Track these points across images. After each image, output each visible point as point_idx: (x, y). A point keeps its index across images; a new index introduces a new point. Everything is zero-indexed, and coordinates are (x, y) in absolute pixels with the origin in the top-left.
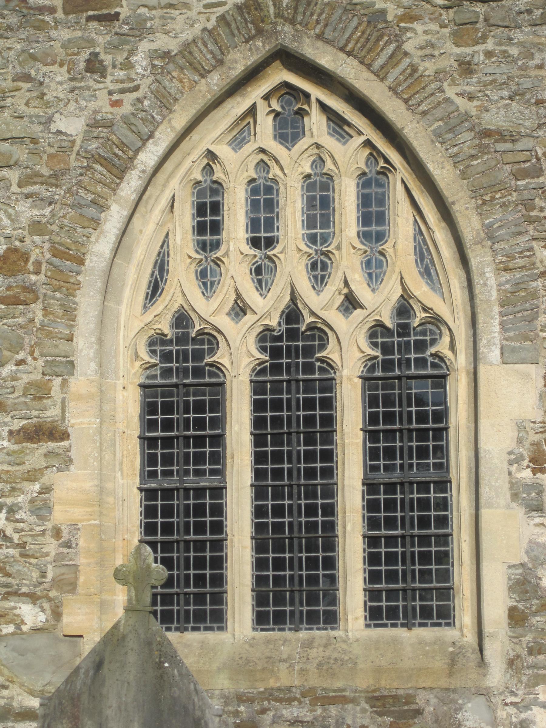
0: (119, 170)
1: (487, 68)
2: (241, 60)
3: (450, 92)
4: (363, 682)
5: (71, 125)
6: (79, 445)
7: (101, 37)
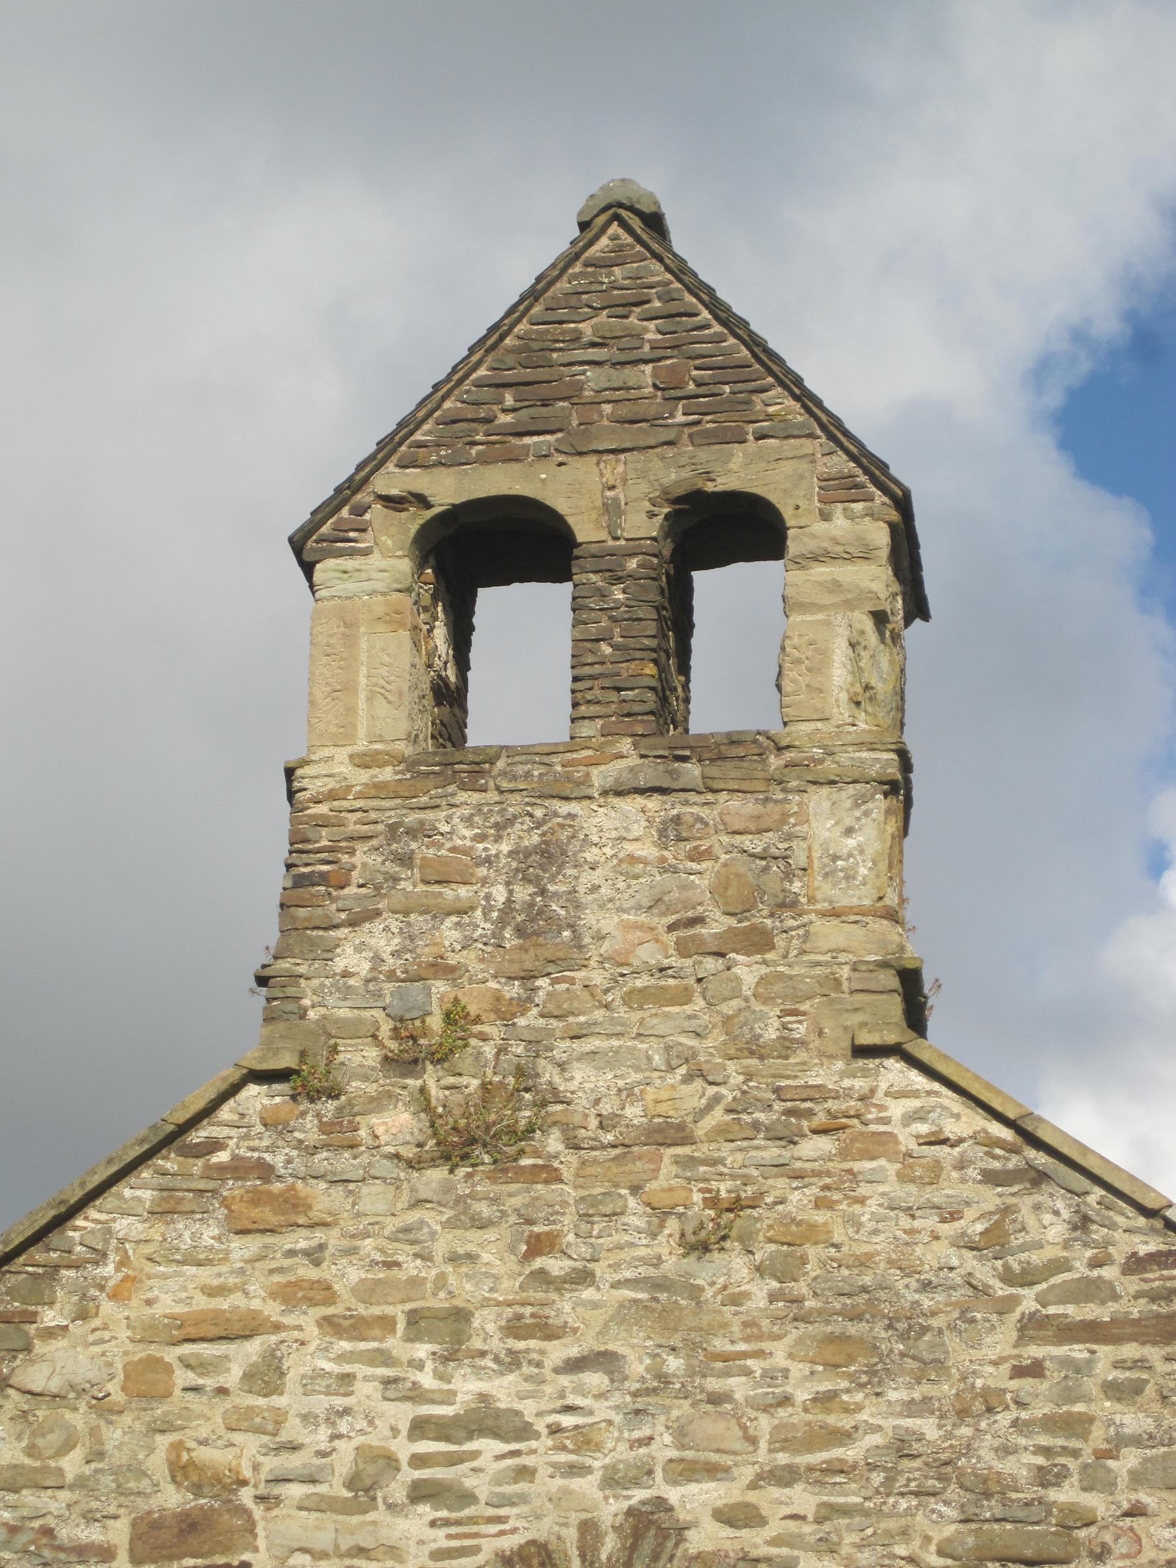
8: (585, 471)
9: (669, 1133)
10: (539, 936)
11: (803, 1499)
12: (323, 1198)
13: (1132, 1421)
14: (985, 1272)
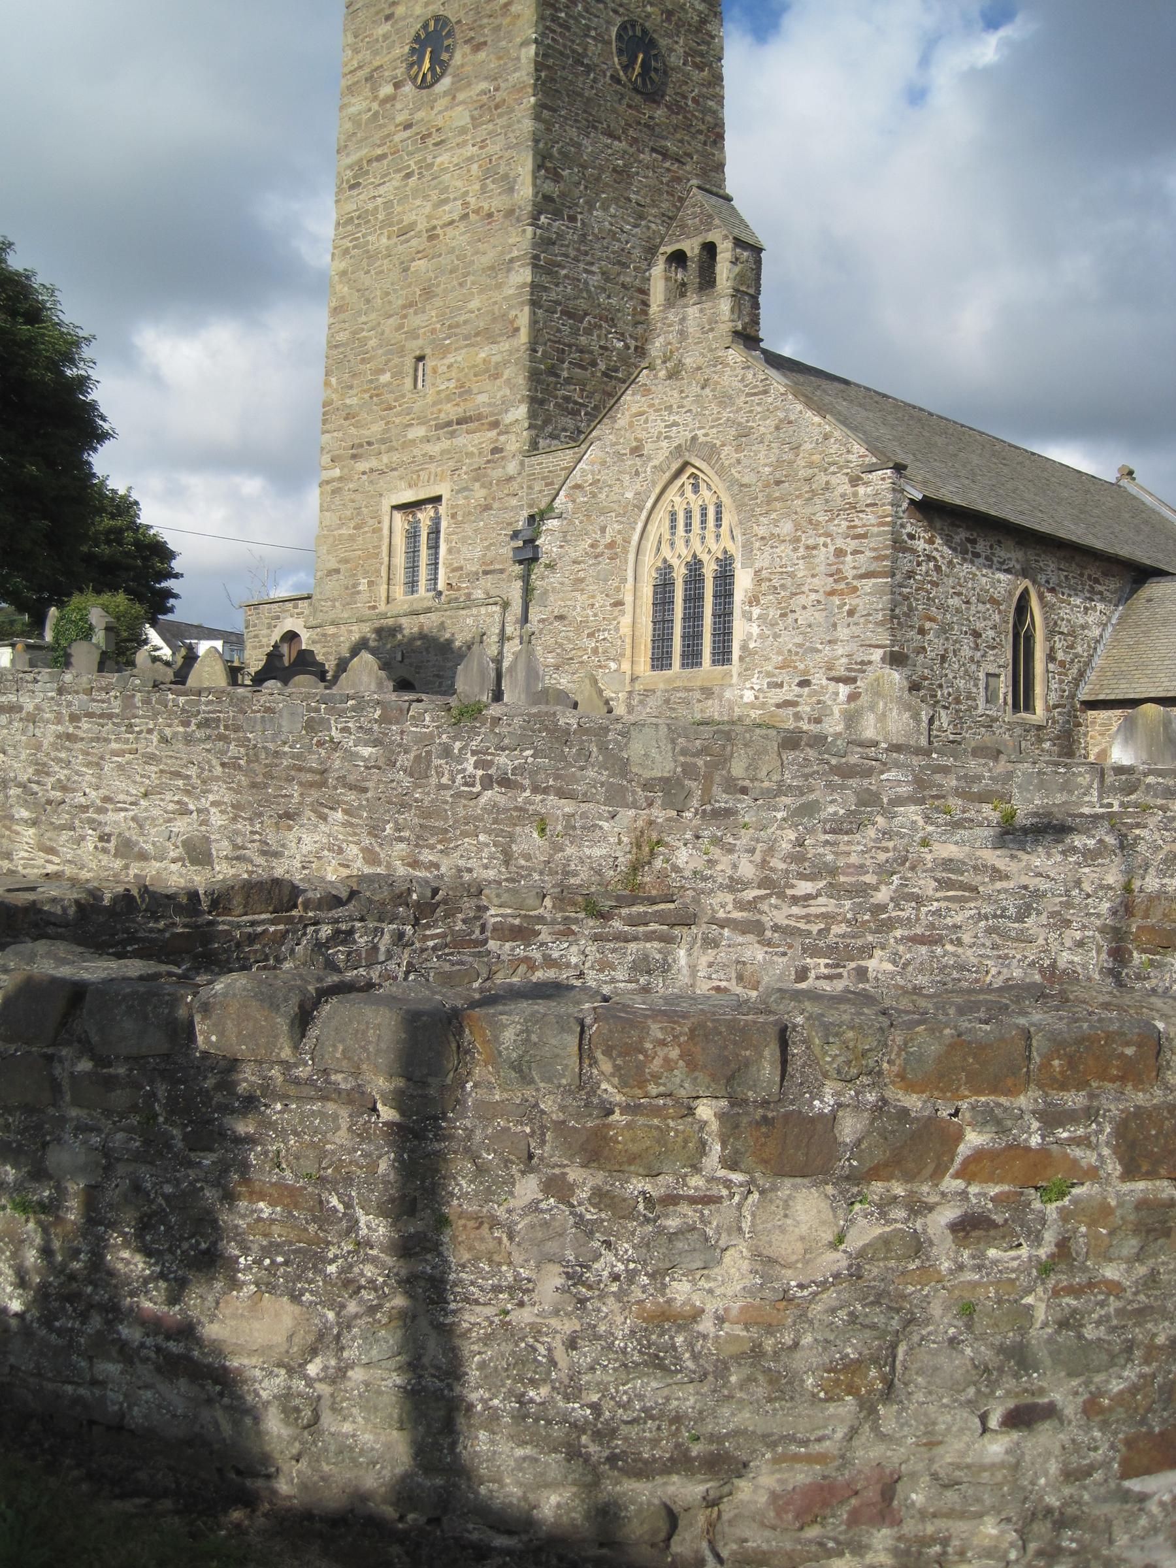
0: (641, 510)
1: (745, 462)
2: (675, 466)
3: (733, 471)
4: (699, 684)
5: (629, 495)
6: (628, 607)
7: (638, 462)
8: (689, 241)
9: (699, 368)
10: (682, 334)
11: (715, 430)
12: (653, 388)
13: (759, 409)
14: (740, 385)
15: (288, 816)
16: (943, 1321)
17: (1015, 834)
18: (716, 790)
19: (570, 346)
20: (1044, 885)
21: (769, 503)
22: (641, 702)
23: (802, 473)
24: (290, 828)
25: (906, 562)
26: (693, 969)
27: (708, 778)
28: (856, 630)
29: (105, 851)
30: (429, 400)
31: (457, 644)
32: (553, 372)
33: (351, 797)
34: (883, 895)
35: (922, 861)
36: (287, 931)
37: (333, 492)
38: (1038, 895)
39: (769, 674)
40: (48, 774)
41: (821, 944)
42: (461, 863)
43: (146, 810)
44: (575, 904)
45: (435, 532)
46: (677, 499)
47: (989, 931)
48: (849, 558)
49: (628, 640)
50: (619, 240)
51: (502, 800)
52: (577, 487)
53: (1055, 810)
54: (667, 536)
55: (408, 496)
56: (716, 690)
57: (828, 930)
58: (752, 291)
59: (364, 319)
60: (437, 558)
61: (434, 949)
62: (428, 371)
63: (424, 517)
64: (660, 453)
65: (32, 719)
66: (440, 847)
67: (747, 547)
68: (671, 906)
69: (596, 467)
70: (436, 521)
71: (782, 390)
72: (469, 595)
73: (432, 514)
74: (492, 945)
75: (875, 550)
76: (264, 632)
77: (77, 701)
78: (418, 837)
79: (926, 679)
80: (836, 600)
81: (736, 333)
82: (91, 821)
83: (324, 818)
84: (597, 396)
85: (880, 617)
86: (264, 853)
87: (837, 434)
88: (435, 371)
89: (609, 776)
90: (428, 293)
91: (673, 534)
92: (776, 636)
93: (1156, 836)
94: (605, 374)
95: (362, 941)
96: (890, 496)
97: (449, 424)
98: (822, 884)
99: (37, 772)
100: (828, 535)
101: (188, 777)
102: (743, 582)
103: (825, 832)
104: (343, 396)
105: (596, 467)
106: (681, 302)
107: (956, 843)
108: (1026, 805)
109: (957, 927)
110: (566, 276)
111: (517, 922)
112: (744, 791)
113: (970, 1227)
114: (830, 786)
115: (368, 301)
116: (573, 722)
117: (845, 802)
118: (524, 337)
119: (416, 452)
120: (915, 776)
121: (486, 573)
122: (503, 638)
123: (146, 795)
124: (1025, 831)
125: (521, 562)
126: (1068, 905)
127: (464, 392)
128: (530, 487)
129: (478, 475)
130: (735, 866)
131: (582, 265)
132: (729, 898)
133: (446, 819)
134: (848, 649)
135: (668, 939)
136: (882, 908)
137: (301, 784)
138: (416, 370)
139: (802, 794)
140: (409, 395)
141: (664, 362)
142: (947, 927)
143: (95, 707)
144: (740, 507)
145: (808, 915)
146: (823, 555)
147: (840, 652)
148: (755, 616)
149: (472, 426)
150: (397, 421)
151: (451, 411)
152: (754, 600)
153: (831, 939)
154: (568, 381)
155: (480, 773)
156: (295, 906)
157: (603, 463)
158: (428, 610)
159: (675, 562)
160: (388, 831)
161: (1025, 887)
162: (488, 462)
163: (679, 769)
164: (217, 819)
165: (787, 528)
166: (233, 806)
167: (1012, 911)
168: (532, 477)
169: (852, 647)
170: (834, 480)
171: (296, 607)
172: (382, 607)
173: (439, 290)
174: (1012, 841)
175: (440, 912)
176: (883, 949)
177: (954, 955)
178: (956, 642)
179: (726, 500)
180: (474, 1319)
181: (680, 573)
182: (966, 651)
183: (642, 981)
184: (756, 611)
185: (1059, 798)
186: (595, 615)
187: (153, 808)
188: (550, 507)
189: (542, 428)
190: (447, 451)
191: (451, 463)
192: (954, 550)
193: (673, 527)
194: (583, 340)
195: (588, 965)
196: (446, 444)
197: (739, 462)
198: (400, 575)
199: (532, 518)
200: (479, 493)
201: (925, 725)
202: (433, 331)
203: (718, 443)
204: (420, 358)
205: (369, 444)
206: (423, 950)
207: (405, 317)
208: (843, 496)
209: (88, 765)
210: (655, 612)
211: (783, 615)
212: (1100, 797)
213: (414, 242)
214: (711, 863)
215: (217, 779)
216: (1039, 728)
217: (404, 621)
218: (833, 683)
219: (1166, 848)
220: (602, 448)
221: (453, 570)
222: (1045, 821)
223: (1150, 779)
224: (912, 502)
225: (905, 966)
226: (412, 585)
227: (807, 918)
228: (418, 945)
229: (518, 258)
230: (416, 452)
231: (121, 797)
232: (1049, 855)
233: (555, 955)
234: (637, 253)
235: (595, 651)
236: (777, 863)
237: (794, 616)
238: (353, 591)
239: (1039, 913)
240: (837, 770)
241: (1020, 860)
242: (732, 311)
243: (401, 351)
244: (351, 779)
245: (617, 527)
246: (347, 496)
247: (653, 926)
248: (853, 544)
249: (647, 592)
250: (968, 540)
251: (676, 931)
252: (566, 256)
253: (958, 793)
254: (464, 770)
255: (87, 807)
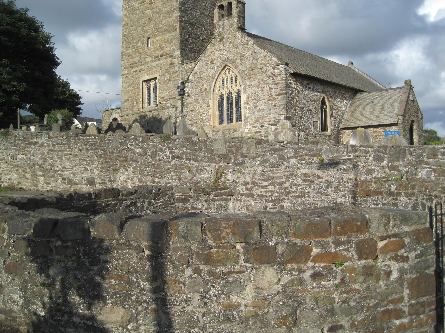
0: (214, 79)
1: (243, 64)
2: (223, 66)
5: (210, 75)
6: (211, 107)
7: (212, 65)
9: (229, 38)
10: (224, 28)
14: (241, 42)
15: (116, 170)
16: (309, 303)
17: (323, 166)
18: (239, 157)
19: (191, 33)
20: (332, 180)
21: (250, 75)
22: (216, 133)
23: (259, 67)
24: (117, 174)
25: (290, 91)
26: (234, 208)
27: (236, 154)
28: (276, 110)
29: (64, 183)
30: (152, 50)
31: (163, 119)
32: (187, 41)
33: (134, 164)
34: (287, 185)
35: (298, 174)
36: (117, 203)
37: (126, 78)
38: (331, 182)
39: (252, 124)
40: (47, 162)
41: (270, 199)
42: (167, 181)
43: (75, 170)
44: (200, 191)
45: (155, 88)
46: (224, 75)
47: (318, 193)
48: (273, 90)
49: (212, 116)
50: (204, 2)
51: (178, 163)
52: (195, 73)
53: (335, 158)
54: (222, 86)
55: (147, 78)
56: (237, 129)
57: (272, 195)
58: (243, 16)
59: (132, 28)
60: (156, 95)
61: (160, 206)
62: (151, 42)
63: (152, 83)
64: (218, 62)
65: (41, 146)
66: (160, 177)
67: (245, 88)
68: (227, 190)
69: (201, 67)
70: (155, 85)
71: (253, 43)
72: (166, 105)
73: (154, 82)
74: (177, 204)
75: (280, 87)
76: (108, 118)
77: (54, 140)
78: (154, 174)
79: (296, 123)
80: (270, 102)
81: (239, 28)
82: (60, 174)
83: (127, 170)
84: (200, 47)
85: (283, 106)
86: (110, 181)
87: (269, 55)
88: (153, 42)
89: (208, 154)
90: (150, 20)
91: (223, 85)
92: (254, 113)
93: (363, 164)
94: (202, 41)
95: (139, 205)
96: (284, 72)
97: (158, 57)
98: (270, 182)
99: (43, 161)
100: (267, 84)
101: (87, 161)
102: (244, 98)
103: (270, 167)
104: (127, 50)
105: (201, 67)
106: (222, 19)
107: (307, 169)
108: (326, 157)
109: (308, 192)
110: (190, 13)
111: (183, 197)
112: (246, 157)
113: (316, 276)
114: (271, 154)
115: (133, 23)
116: (197, 139)
117: (275, 159)
118: (178, 31)
119: (149, 65)
120: (295, 150)
121: (170, 99)
122: (176, 117)
123: (75, 166)
124: (326, 164)
125: (180, 95)
126: (339, 185)
127: (162, 47)
128: (182, 74)
129: (167, 71)
130: (245, 178)
131: (194, 10)
132: (244, 187)
133: (162, 169)
134: (274, 116)
135: (227, 200)
136: (287, 188)
137: (120, 161)
138: (148, 42)
139: (263, 157)
140: (146, 49)
141: (219, 37)
142: (306, 193)
143: (59, 142)
144: (242, 77)
145: (266, 191)
146: (266, 90)
147: (272, 117)
148: (247, 108)
149: (164, 57)
150: (143, 56)
151: (158, 53)
152: (247, 103)
153: (273, 198)
154: (191, 43)
155: (171, 155)
156: (119, 196)
157: (202, 66)
158: (154, 110)
159: (224, 93)
160: (145, 173)
161: (327, 180)
162: (170, 67)
163: (228, 152)
164: (96, 172)
165: (255, 82)
166: (100, 168)
167: (324, 187)
168: (182, 71)
169: (275, 115)
170: (268, 68)
171: (116, 111)
172: (141, 110)
173: (153, 19)
174: (323, 167)
175: (161, 195)
176: (288, 200)
177: (308, 200)
178: (305, 113)
179: (238, 75)
180: (175, 310)
181: (226, 97)
182: (308, 115)
183: (220, 212)
184: (248, 106)
185: (336, 155)
186: (202, 109)
187: (78, 170)
188: (188, 79)
189: (184, 57)
190: (158, 65)
191: (159, 68)
192: (303, 87)
193: (223, 83)
194: (195, 31)
195: (204, 208)
196: (157, 62)
197: (241, 64)
198: (146, 100)
199: (183, 83)
200: (167, 76)
201: (297, 136)
202: (152, 30)
203: (235, 59)
204: (149, 38)
205: (135, 63)
206: (157, 206)
207: (144, 27)
208: (271, 72)
209: (58, 158)
210: (219, 108)
211: (256, 107)
212: (347, 154)
213: (146, 5)
214: (238, 178)
215: (96, 160)
216: (329, 136)
217: (148, 114)
218: (270, 126)
219: (366, 167)
220: (202, 62)
221: (161, 98)
222: (332, 161)
223: (361, 148)
224: (291, 73)
225: (294, 204)
226: (149, 103)
227: (266, 192)
228: (155, 205)
229: (176, 9)
230: (149, 65)
231: (68, 167)
232: (333, 171)
233: (195, 206)
234: (210, 6)
235: (202, 120)
236: (257, 177)
237: (259, 107)
238: (132, 105)
239: (331, 188)
240: (272, 150)
241: (325, 173)
242: (237, 22)
243: (143, 37)
244: (134, 158)
245: (207, 84)
246: (130, 78)
247: (222, 196)
248: (274, 86)
249: (217, 102)
250: (307, 84)
251: (229, 198)
252: (190, 8)
253: (307, 155)
254: (166, 155)
255: (58, 170)
